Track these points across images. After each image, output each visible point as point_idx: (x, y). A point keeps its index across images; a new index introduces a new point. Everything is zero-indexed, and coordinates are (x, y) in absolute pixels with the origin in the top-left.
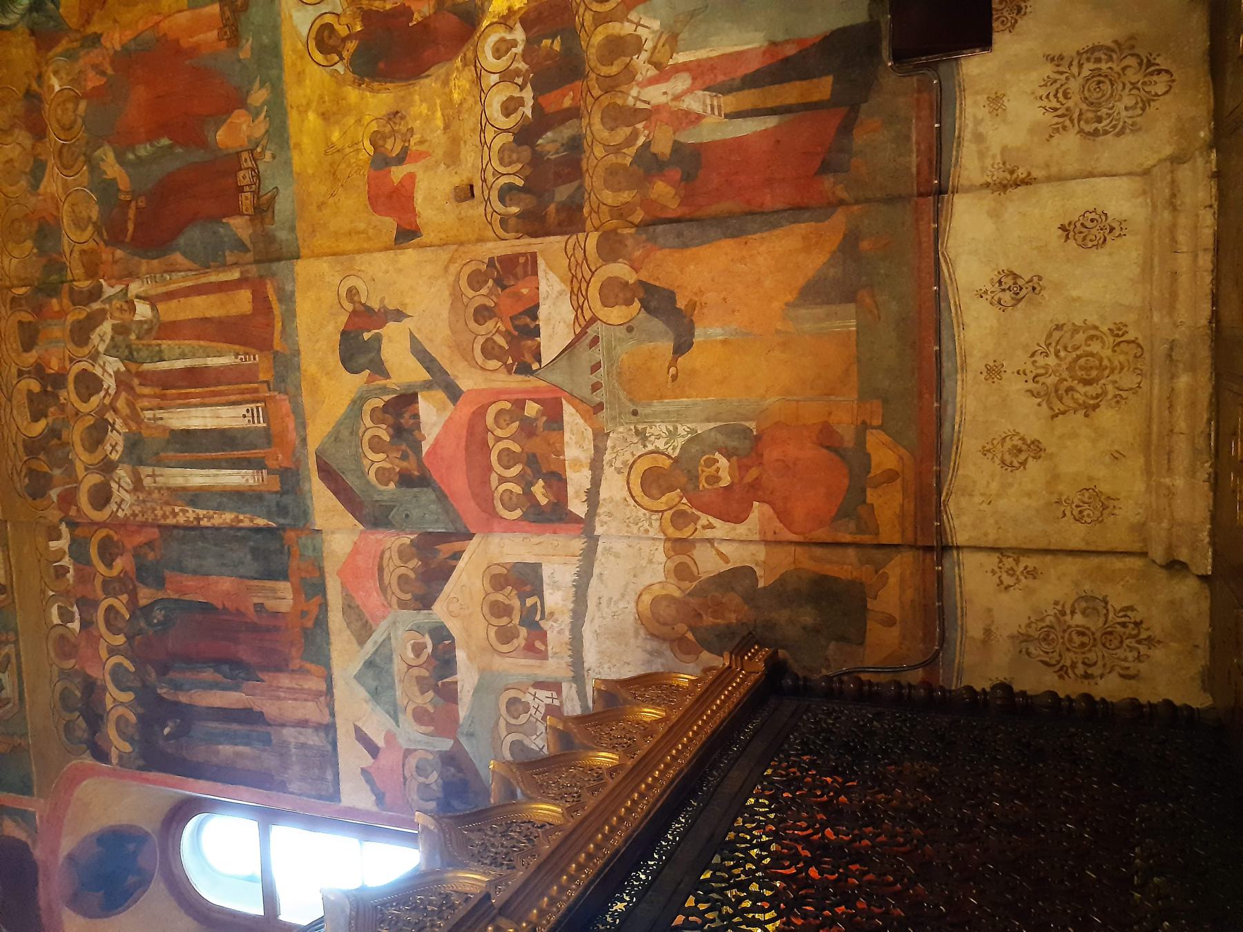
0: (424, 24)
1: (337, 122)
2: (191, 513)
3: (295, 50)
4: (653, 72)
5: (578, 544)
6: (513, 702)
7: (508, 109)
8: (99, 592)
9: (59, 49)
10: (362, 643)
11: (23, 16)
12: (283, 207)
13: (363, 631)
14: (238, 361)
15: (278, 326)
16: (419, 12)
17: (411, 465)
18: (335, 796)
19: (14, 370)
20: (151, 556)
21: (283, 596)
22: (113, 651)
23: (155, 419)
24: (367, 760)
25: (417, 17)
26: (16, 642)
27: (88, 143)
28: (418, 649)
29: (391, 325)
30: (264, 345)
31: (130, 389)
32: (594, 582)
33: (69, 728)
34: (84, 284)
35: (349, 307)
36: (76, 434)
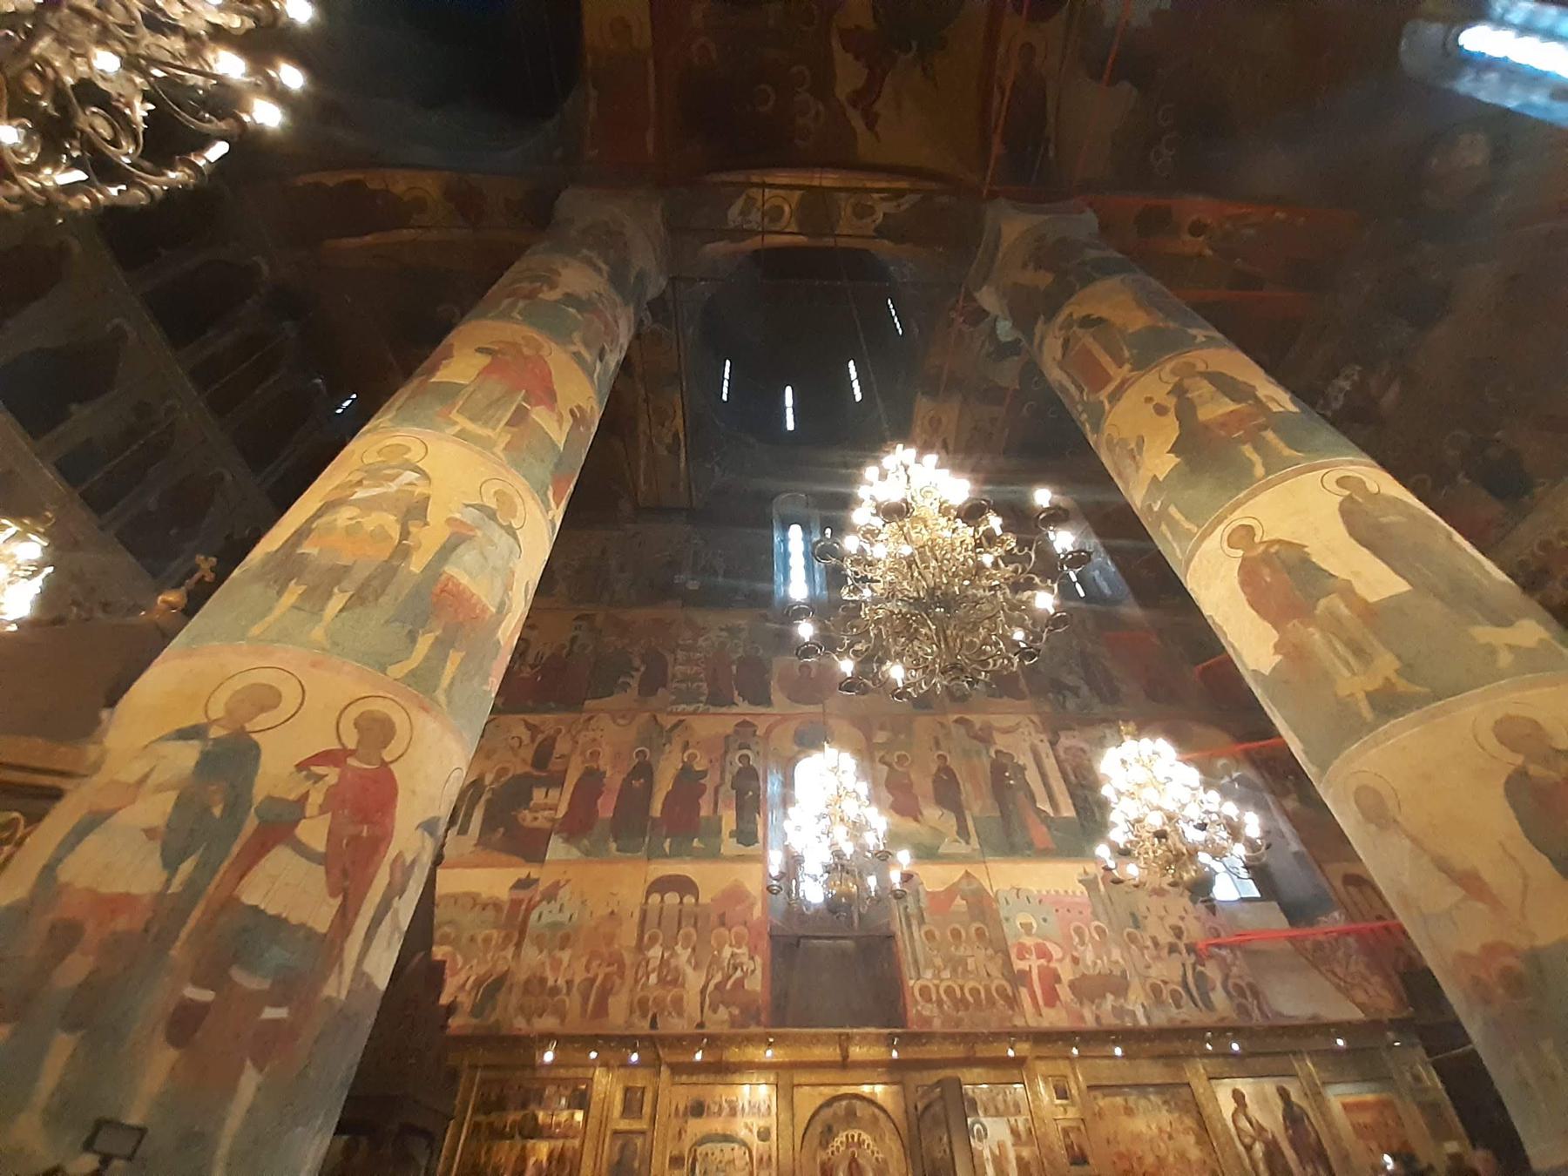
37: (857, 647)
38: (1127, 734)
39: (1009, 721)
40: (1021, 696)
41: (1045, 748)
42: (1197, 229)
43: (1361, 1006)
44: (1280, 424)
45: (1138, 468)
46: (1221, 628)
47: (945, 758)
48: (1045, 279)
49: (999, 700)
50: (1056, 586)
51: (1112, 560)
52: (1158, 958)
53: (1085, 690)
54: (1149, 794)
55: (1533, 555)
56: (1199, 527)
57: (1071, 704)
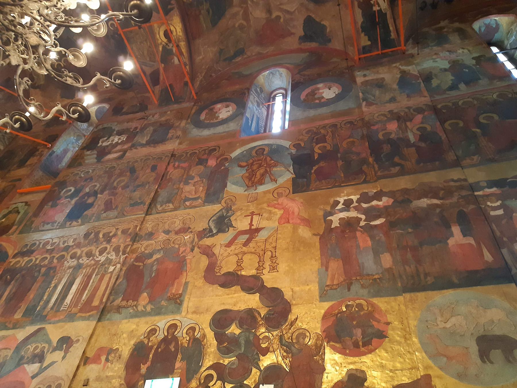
0: (139, 369)
1: (128, 335)
2: (53, 285)
3: (155, 320)
8: (52, 255)
9: (196, 238)
11: (209, 226)
12: (116, 316)
14: (82, 301)
15: (83, 315)
16: (143, 368)
17: (25, 360)
19: (119, 227)
20: (52, 272)
21: (18, 316)
22: (36, 259)
23: (83, 273)
25: (142, 366)
26: (56, 229)
27: (166, 248)
30: (81, 311)
31: (94, 265)
33: (27, 245)
35: (74, 340)
36: (93, 248)
55: (40, 243)
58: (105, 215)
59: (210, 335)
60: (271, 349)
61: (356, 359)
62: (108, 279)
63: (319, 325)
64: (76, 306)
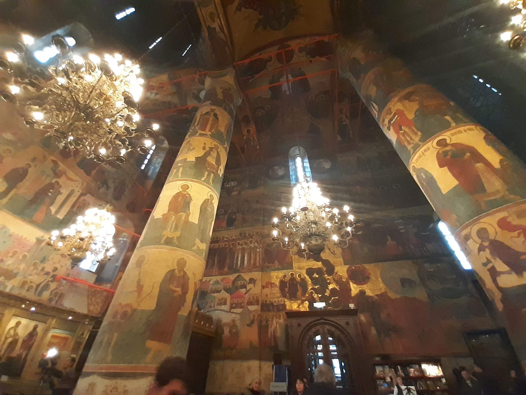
0: (285, 290)
4: (277, 321)
5: (228, 310)
6: (212, 301)
7: (275, 301)
10: (220, 280)
13: (222, 280)
18: (205, 277)
21: (226, 269)
22: (222, 245)
24: (208, 281)
25: (286, 289)
28: (219, 288)
29: (253, 285)
32: (224, 312)
34: (262, 242)
36: (246, 240)
37: (29, 87)
38: (107, 208)
39: (74, 177)
40: (88, 173)
41: (77, 194)
42: (248, 131)
43: (89, 311)
44: (216, 175)
45: (186, 153)
46: (159, 201)
47: (30, 166)
48: (220, 96)
49: (80, 170)
50: (130, 150)
51: (160, 169)
52: (38, 274)
53: (111, 190)
54: (92, 228)
55: (220, 237)
56: (181, 177)
57: (101, 190)
58: (244, 225)
59: (307, 278)
60: (331, 283)
61: (361, 286)
62: (258, 254)
63: (346, 274)
64: (250, 266)
